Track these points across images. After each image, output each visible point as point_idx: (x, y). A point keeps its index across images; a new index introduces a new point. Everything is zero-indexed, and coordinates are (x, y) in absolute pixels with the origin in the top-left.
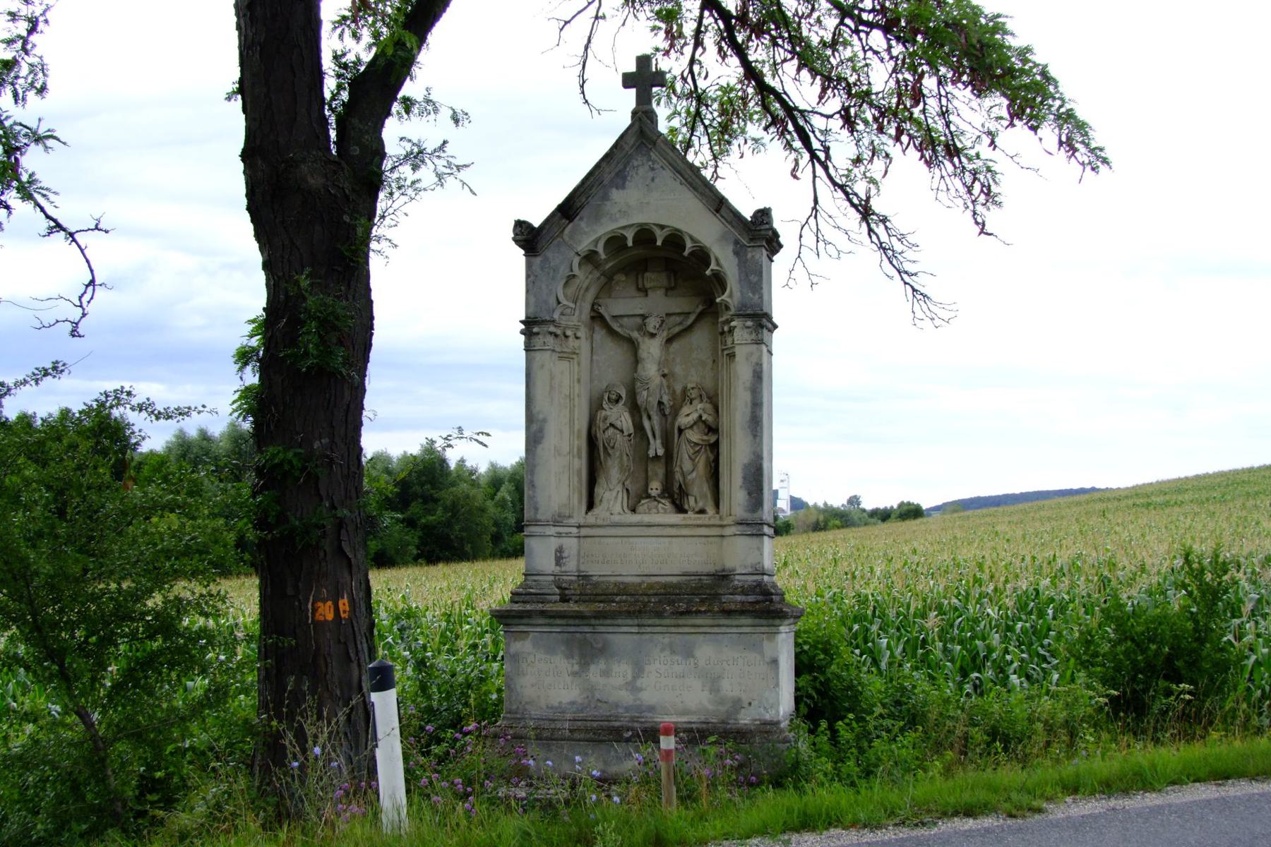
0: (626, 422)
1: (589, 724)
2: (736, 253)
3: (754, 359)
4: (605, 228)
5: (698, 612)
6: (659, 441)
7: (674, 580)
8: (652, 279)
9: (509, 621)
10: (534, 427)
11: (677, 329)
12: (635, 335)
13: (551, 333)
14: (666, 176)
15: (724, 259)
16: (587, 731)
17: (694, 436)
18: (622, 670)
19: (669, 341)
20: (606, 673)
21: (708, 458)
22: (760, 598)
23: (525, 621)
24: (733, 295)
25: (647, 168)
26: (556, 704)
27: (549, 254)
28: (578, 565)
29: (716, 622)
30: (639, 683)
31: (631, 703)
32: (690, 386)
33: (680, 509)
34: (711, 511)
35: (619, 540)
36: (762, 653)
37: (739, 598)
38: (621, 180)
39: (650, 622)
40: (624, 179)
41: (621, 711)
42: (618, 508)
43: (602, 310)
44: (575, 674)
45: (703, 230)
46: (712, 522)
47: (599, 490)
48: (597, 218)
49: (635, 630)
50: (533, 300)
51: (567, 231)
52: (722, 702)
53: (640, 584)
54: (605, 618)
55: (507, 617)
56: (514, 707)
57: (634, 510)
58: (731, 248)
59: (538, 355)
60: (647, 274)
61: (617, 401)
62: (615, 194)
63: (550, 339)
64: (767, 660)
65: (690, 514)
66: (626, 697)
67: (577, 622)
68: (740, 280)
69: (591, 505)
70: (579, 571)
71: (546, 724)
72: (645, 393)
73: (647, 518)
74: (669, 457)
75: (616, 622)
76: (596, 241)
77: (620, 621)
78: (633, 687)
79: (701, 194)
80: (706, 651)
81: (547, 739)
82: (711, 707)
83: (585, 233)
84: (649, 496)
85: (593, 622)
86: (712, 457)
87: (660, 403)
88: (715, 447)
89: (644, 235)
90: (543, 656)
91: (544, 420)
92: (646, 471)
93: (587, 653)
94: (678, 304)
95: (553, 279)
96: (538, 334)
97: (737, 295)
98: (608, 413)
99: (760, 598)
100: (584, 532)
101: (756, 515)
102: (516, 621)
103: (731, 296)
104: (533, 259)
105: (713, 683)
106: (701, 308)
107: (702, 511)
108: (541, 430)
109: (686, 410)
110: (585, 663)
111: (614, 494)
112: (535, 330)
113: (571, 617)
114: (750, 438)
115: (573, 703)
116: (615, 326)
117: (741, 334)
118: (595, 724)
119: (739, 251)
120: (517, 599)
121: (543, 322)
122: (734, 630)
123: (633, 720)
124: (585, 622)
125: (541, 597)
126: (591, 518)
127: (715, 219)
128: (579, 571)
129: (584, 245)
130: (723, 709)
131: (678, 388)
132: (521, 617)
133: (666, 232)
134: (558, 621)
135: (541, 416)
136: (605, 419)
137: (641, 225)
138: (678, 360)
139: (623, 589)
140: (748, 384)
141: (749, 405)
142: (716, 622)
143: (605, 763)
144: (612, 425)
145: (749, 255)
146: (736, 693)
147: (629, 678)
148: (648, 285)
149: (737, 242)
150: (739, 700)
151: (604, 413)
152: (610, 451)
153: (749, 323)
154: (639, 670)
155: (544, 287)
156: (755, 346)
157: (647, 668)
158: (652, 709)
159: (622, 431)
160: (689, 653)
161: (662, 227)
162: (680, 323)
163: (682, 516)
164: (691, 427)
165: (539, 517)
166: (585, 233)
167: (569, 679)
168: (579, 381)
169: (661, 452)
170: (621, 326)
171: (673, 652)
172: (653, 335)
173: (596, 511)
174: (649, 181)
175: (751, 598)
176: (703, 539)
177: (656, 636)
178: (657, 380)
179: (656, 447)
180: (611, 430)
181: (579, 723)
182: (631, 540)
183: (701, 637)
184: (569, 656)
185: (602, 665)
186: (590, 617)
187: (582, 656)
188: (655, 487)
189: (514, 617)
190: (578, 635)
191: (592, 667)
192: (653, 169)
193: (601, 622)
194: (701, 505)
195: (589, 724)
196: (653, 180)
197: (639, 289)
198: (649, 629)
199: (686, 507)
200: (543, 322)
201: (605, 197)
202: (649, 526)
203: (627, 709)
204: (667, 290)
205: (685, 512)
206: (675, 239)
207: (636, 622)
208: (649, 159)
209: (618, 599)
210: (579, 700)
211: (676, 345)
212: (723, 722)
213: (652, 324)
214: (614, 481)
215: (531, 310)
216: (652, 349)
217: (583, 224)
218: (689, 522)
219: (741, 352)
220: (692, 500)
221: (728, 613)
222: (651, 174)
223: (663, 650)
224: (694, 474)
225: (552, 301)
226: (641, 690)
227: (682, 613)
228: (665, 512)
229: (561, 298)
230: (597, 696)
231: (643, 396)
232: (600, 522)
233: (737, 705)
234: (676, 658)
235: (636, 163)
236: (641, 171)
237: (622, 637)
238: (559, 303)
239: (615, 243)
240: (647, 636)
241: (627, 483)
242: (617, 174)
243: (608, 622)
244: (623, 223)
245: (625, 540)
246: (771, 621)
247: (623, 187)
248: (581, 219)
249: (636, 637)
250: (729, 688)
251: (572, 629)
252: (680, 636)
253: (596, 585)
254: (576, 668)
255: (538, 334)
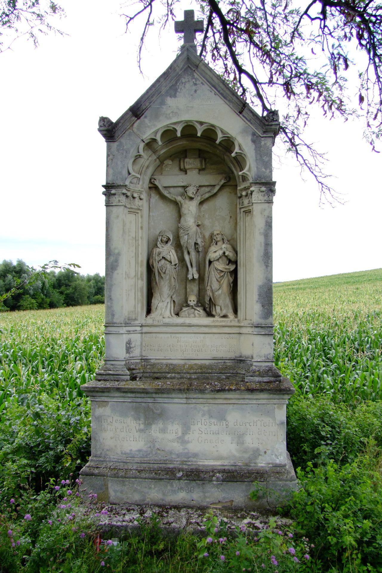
0: (173, 256)
1: (151, 465)
2: (253, 141)
3: (266, 213)
4: (162, 124)
5: (230, 390)
6: (195, 269)
7: (207, 362)
8: (191, 163)
9: (94, 394)
10: (112, 259)
11: (207, 195)
12: (179, 199)
13: (124, 194)
14: (205, 89)
15: (244, 144)
16: (151, 471)
17: (221, 266)
18: (174, 429)
19: (201, 203)
20: (163, 431)
21: (229, 280)
22: (272, 379)
23: (106, 394)
24: (251, 168)
25: (192, 83)
26: (128, 451)
27: (123, 140)
28: (141, 352)
29: (242, 397)
30: (186, 438)
31: (181, 451)
32: (215, 233)
33: (209, 314)
34: (231, 315)
35: (169, 335)
36: (274, 418)
37: (257, 379)
38: (173, 91)
39: (195, 396)
40: (176, 90)
41: (174, 456)
42: (168, 313)
43: (157, 183)
44: (141, 431)
45: (230, 124)
46: (232, 324)
47: (154, 302)
48: (156, 117)
49: (184, 401)
50: (111, 171)
51: (136, 125)
52: (245, 451)
53: (184, 365)
54: (162, 393)
55: (93, 391)
56: (99, 453)
57: (177, 314)
58: (250, 138)
59: (114, 209)
60: (187, 160)
61: (167, 242)
62: (170, 101)
63: (123, 198)
64: (278, 422)
65: (217, 318)
66: (177, 447)
67: (143, 395)
68: (257, 160)
69: (149, 311)
70: (141, 356)
71: (121, 466)
72: (186, 237)
73: (188, 321)
74: (201, 279)
75: (170, 396)
76: (156, 132)
77: (173, 396)
78: (182, 440)
79: (229, 101)
80: (234, 416)
81: (122, 477)
82: (237, 454)
83: (148, 127)
84: (188, 306)
85: (154, 395)
86: (231, 280)
87: (196, 244)
88: (235, 273)
89: (189, 129)
90: (119, 418)
91: (119, 254)
92: (186, 288)
93: (150, 417)
94: (207, 179)
95: (126, 157)
96: (114, 194)
97: (254, 170)
98: (161, 250)
99: (272, 379)
100: (145, 329)
101: (268, 321)
102: (100, 394)
103: (249, 170)
104: (112, 144)
105: (239, 438)
106: (223, 182)
107: (225, 316)
108: (117, 261)
109: (213, 248)
110: (148, 424)
111: (165, 304)
112: (113, 191)
113: (138, 392)
114: (264, 267)
115: (140, 451)
116: (165, 193)
117: (257, 197)
118: (156, 466)
119: (256, 139)
120: (99, 377)
121: (119, 186)
122: (254, 402)
123: (183, 463)
124: (149, 395)
125: (116, 377)
126: (149, 320)
127: (238, 118)
128: (141, 356)
129: (147, 135)
130: (246, 456)
131: (207, 235)
132: (103, 392)
133: (204, 127)
134: (129, 395)
135: (116, 251)
136: (159, 254)
137: (187, 122)
138: (207, 216)
139: (173, 369)
140: (262, 231)
141: (263, 244)
142: (242, 397)
143: (164, 494)
144: (163, 258)
145: (263, 143)
146: (255, 445)
147: (180, 434)
148: (187, 167)
149: (254, 134)
150: (258, 450)
151: (158, 250)
152: (163, 275)
153: (263, 189)
154: (186, 429)
155: (119, 163)
156: (267, 204)
157: (192, 427)
158: (196, 455)
159: (171, 262)
160: (222, 418)
161: (201, 123)
162: (209, 192)
163: (211, 319)
164: (218, 260)
165: (115, 321)
166: (148, 127)
167: (137, 435)
168: (142, 228)
169: (196, 276)
170: (170, 193)
171: (211, 417)
172: (191, 199)
173: (152, 315)
174: (193, 92)
175: (266, 379)
176: (227, 336)
177: (198, 405)
178: (194, 228)
179: (193, 273)
180: (163, 261)
181: (145, 465)
182: (177, 335)
183: (231, 406)
184: (137, 418)
185: (161, 425)
186: (152, 393)
187: (146, 418)
188: (193, 299)
189: (97, 392)
190: (143, 404)
191: (153, 426)
192: (195, 84)
193: (160, 395)
194: (224, 312)
195: (151, 465)
196: (196, 91)
197: (181, 170)
198: (194, 401)
199: (214, 313)
200: (119, 186)
201: (163, 103)
202: (190, 326)
203: (178, 455)
204: (200, 170)
205: (213, 316)
206: (210, 133)
207: (185, 396)
208: (193, 78)
209: (169, 375)
210: (145, 449)
211: (205, 206)
212: (247, 465)
213: (191, 191)
214: (165, 295)
215: (110, 179)
216: (190, 208)
217: (147, 121)
218: (217, 324)
219: (257, 209)
220: (218, 308)
221: (251, 391)
222: (194, 88)
223: (203, 415)
224: (220, 291)
225: (125, 172)
226: (188, 442)
227: (218, 391)
228: (200, 316)
229: (131, 171)
230: (157, 446)
231: (184, 240)
232: (156, 323)
233: (256, 453)
234: (213, 420)
235: (184, 81)
236: (187, 85)
237: (175, 405)
238: (129, 174)
239: (168, 134)
240: (192, 406)
241: (173, 297)
242: (170, 88)
243: (165, 396)
244: (174, 120)
245: (173, 335)
246: (281, 396)
247: (175, 96)
248: (146, 117)
249: (186, 405)
250: (251, 442)
251: (139, 400)
252: (216, 406)
253: (153, 365)
254: (142, 426)
255: (114, 194)
